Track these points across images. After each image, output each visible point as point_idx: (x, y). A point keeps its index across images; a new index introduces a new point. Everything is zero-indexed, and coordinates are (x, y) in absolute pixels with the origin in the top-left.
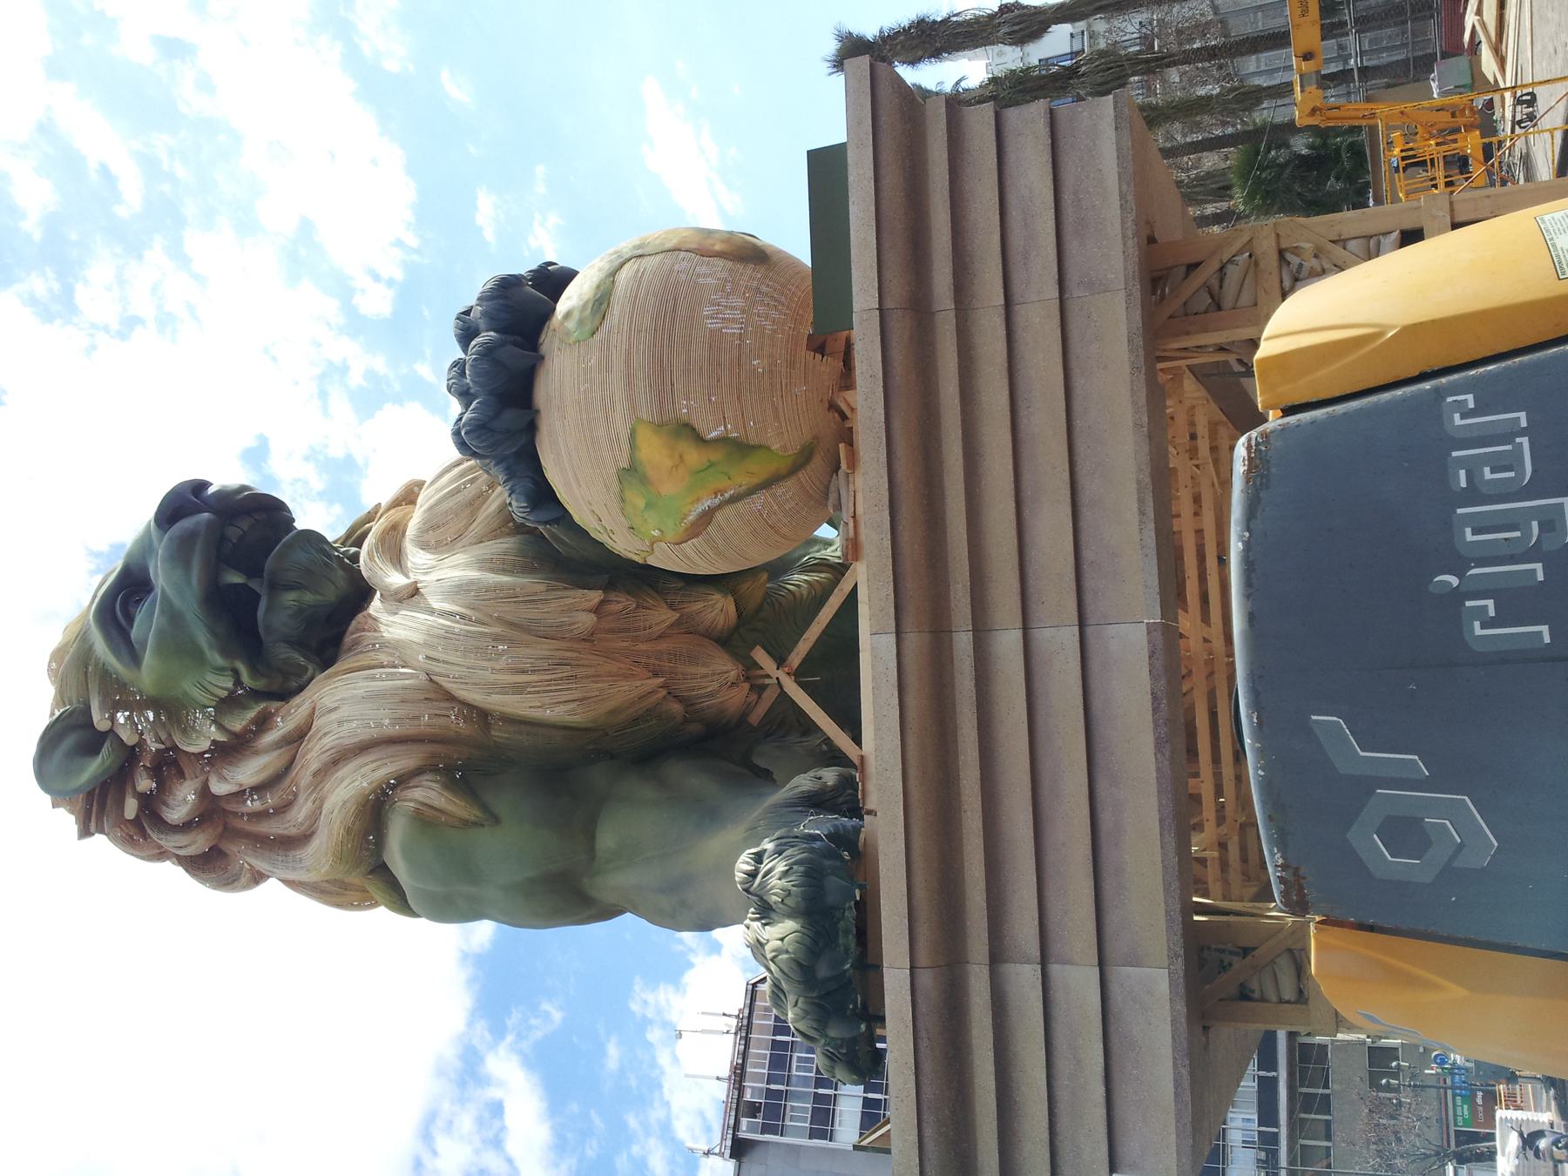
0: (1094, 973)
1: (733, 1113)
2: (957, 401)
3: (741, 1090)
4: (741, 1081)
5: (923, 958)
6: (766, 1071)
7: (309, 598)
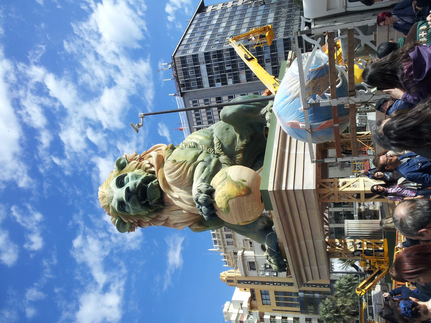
1: (179, 88)
2: (292, 222)
3: (179, 82)
4: (178, 80)
5: (295, 271)
6: (183, 76)
7: (157, 199)
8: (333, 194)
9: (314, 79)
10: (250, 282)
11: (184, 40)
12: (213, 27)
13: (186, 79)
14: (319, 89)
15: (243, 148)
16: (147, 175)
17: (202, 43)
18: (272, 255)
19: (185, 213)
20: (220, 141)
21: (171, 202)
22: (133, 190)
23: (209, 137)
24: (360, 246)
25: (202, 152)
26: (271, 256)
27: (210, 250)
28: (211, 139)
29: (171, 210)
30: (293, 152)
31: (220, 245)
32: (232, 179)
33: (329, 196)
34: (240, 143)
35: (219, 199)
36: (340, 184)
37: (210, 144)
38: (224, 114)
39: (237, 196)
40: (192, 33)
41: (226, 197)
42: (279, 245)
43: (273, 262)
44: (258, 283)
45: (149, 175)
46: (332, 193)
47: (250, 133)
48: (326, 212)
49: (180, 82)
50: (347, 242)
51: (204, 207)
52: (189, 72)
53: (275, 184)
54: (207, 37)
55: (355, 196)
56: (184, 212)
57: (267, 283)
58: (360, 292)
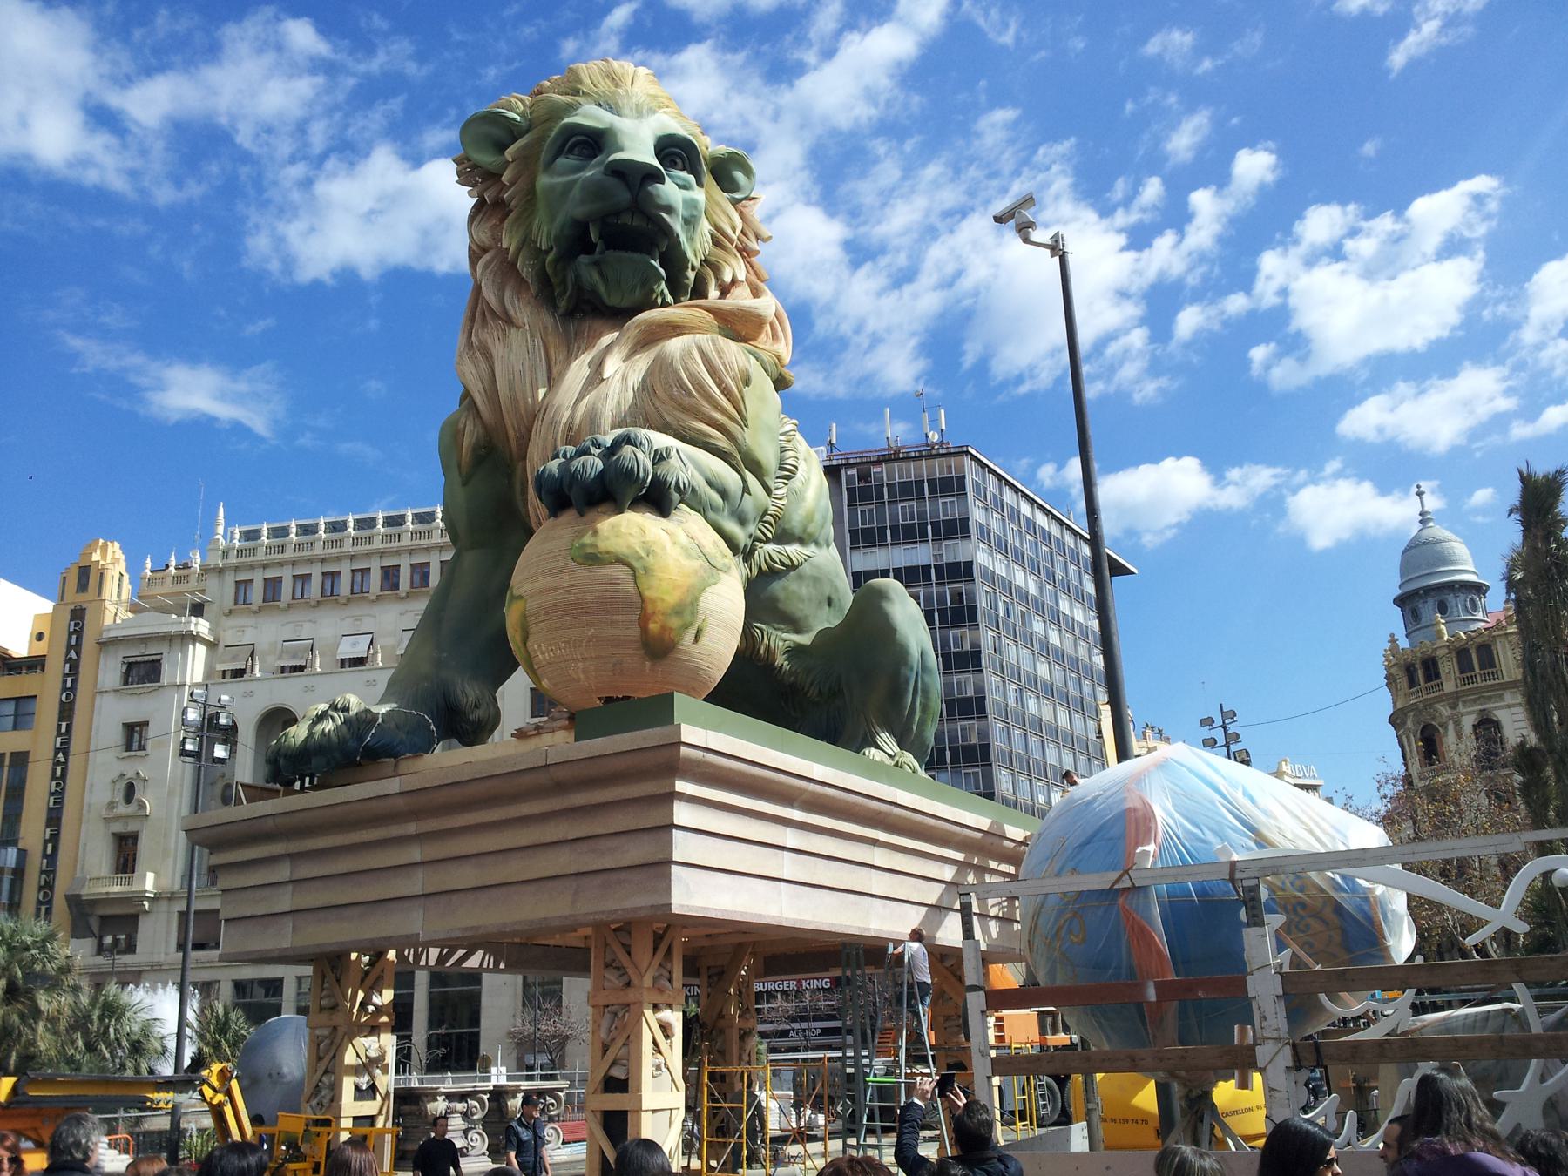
0: (287, 909)
1: (858, 460)
3: (878, 462)
5: (279, 820)
6: (897, 480)
7: (602, 289)
8: (628, 984)
9: (1338, 908)
10: (74, 656)
11: (1015, 496)
12: (1049, 601)
13: (885, 489)
14: (1297, 927)
15: (762, 652)
16: (690, 265)
17: (1003, 558)
18: (349, 729)
19: (534, 396)
20: (797, 567)
21: (583, 346)
22: (650, 196)
23: (811, 529)
24: (364, 1087)
25: (768, 491)
26: (347, 722)
27: (221, 510)
28: (805, 537)
29: (551, 339)
30: (791, 838)
31: (240, 551)
32: (708, 589)
33: (618, 969)
34: (781, 643)
35: (635, 530)
36: (666, 1015)
37: (786, 527)
38: (892, 595)
39: (642, 598)
40: (1035, 524)
41: (641, 558)
42: (387, 760)
43: (319, 728)
44: (70, 690)
45: (691, 275)
46: (635, 980)
47: (813, 688)
48: (487, 958)
49: (879, 469)
50: (382, 1036)
51: (600, 465)
52: (911, 503)
53: (699, 754)
54: (1019, 578)
55: (618, 1073)
56: (542, 392)
57: (64, 725)
58: (215, 1081)
